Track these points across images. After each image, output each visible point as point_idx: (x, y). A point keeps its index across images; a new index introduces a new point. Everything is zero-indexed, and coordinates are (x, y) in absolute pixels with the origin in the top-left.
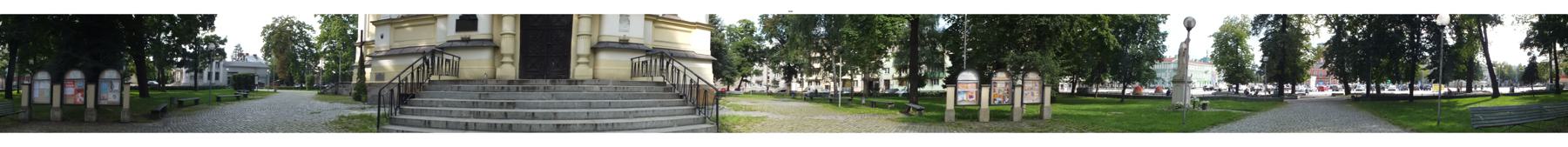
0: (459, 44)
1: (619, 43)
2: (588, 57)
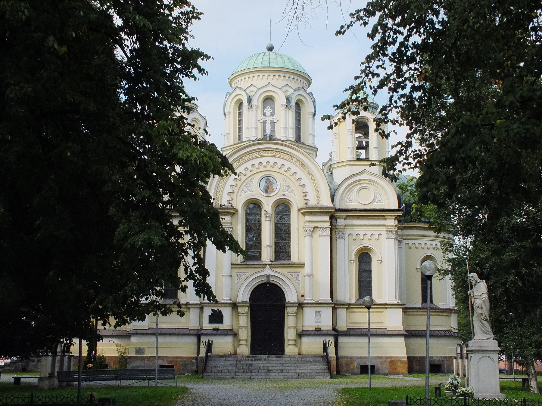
1: (315, 330)
2: (295, 340)
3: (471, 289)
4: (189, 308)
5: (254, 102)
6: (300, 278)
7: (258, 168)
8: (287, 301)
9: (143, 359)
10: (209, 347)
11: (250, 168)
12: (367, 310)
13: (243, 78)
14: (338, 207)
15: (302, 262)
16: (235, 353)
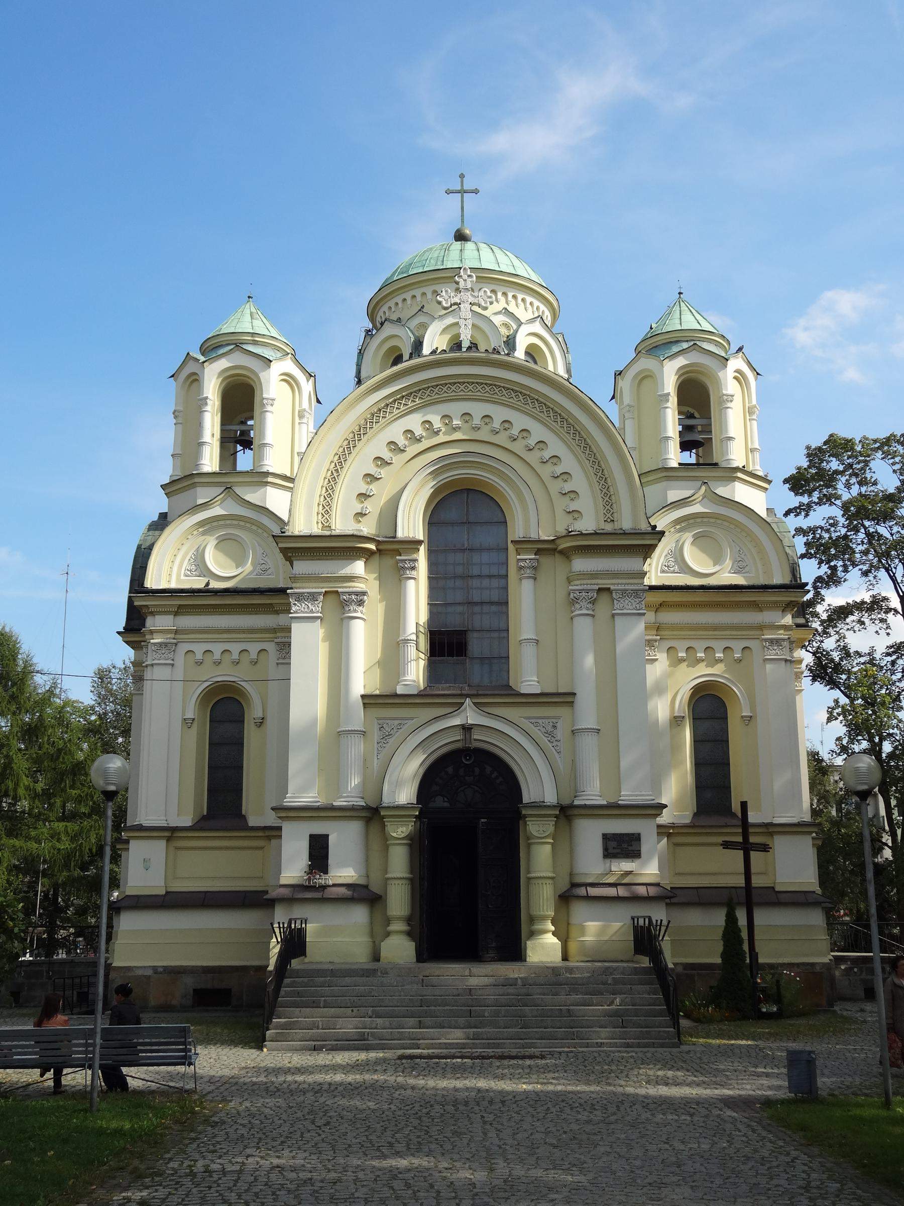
8: (526, 800)
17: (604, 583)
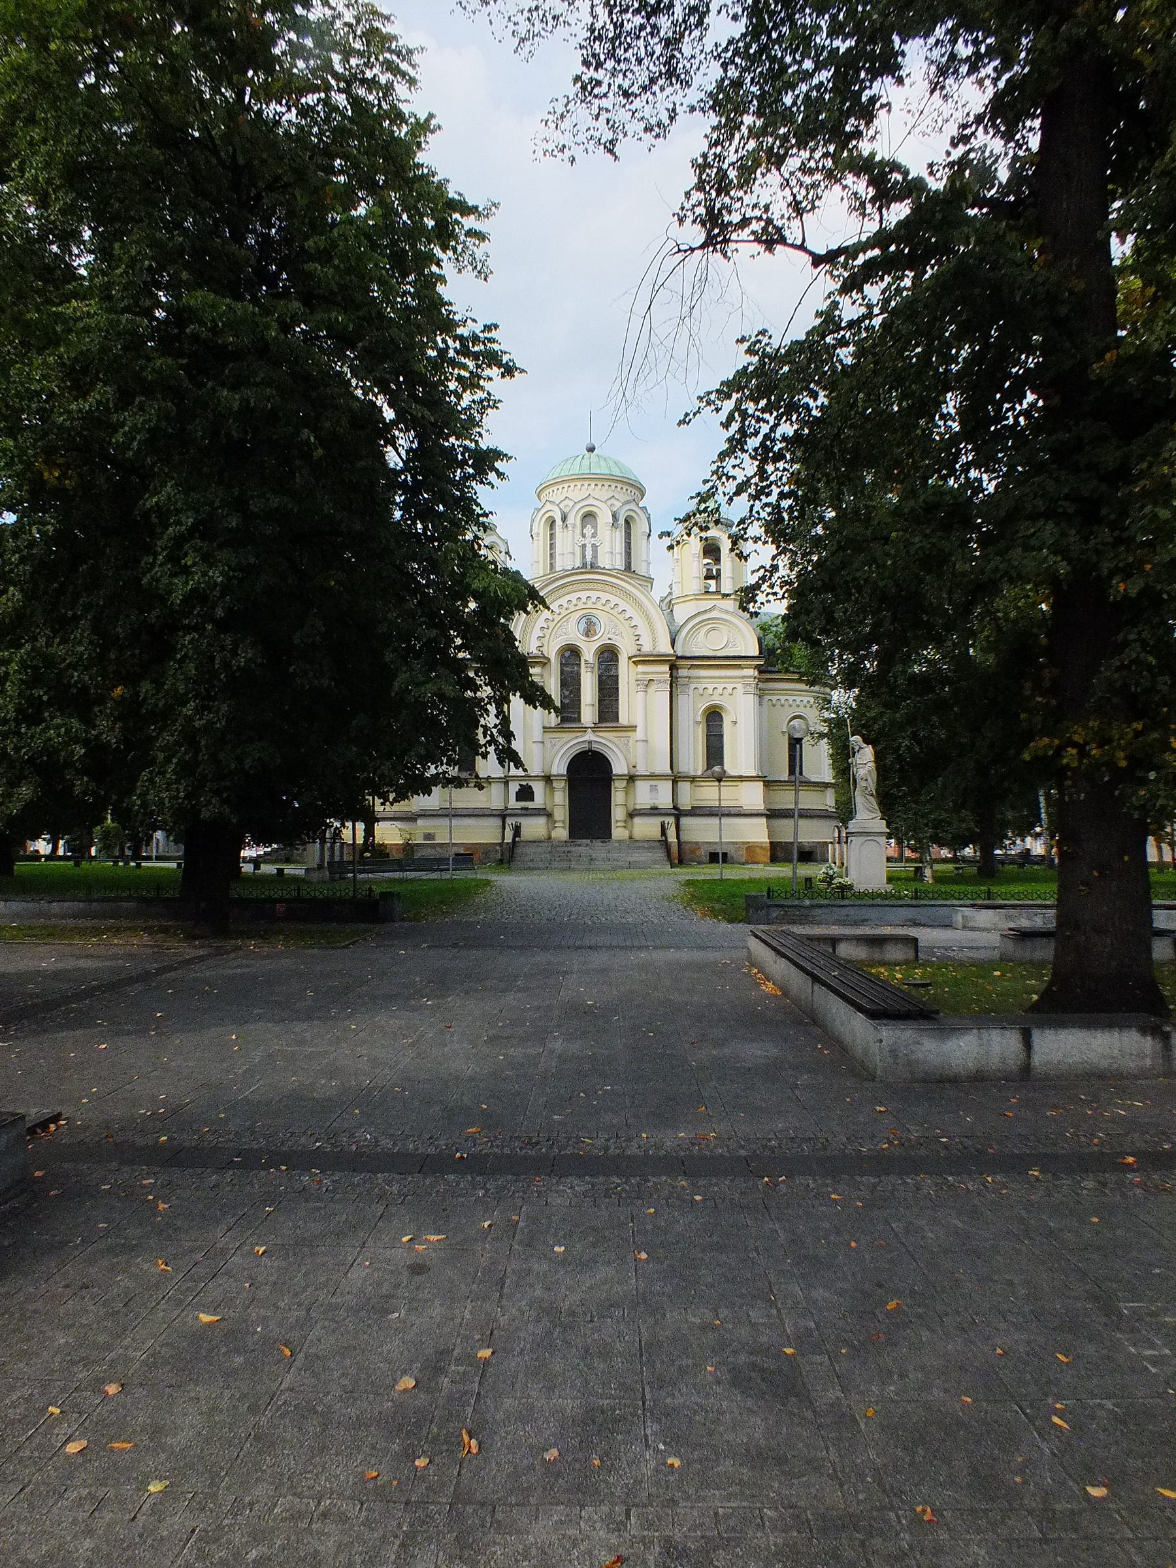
0: (519, 812)
2: (625, 821)
3: (854, 756)
4: (490, 783)
5: (570, 521)
6: (630, 744)
7: (575, 605)
9: (434, 846)
10: (517, 830)
11: (566, 606)
12: (717, 783)
13: (555, 488)
14: (680, 654)
15: (633, 724)
16: (550, 838)
17: (651, 677)
